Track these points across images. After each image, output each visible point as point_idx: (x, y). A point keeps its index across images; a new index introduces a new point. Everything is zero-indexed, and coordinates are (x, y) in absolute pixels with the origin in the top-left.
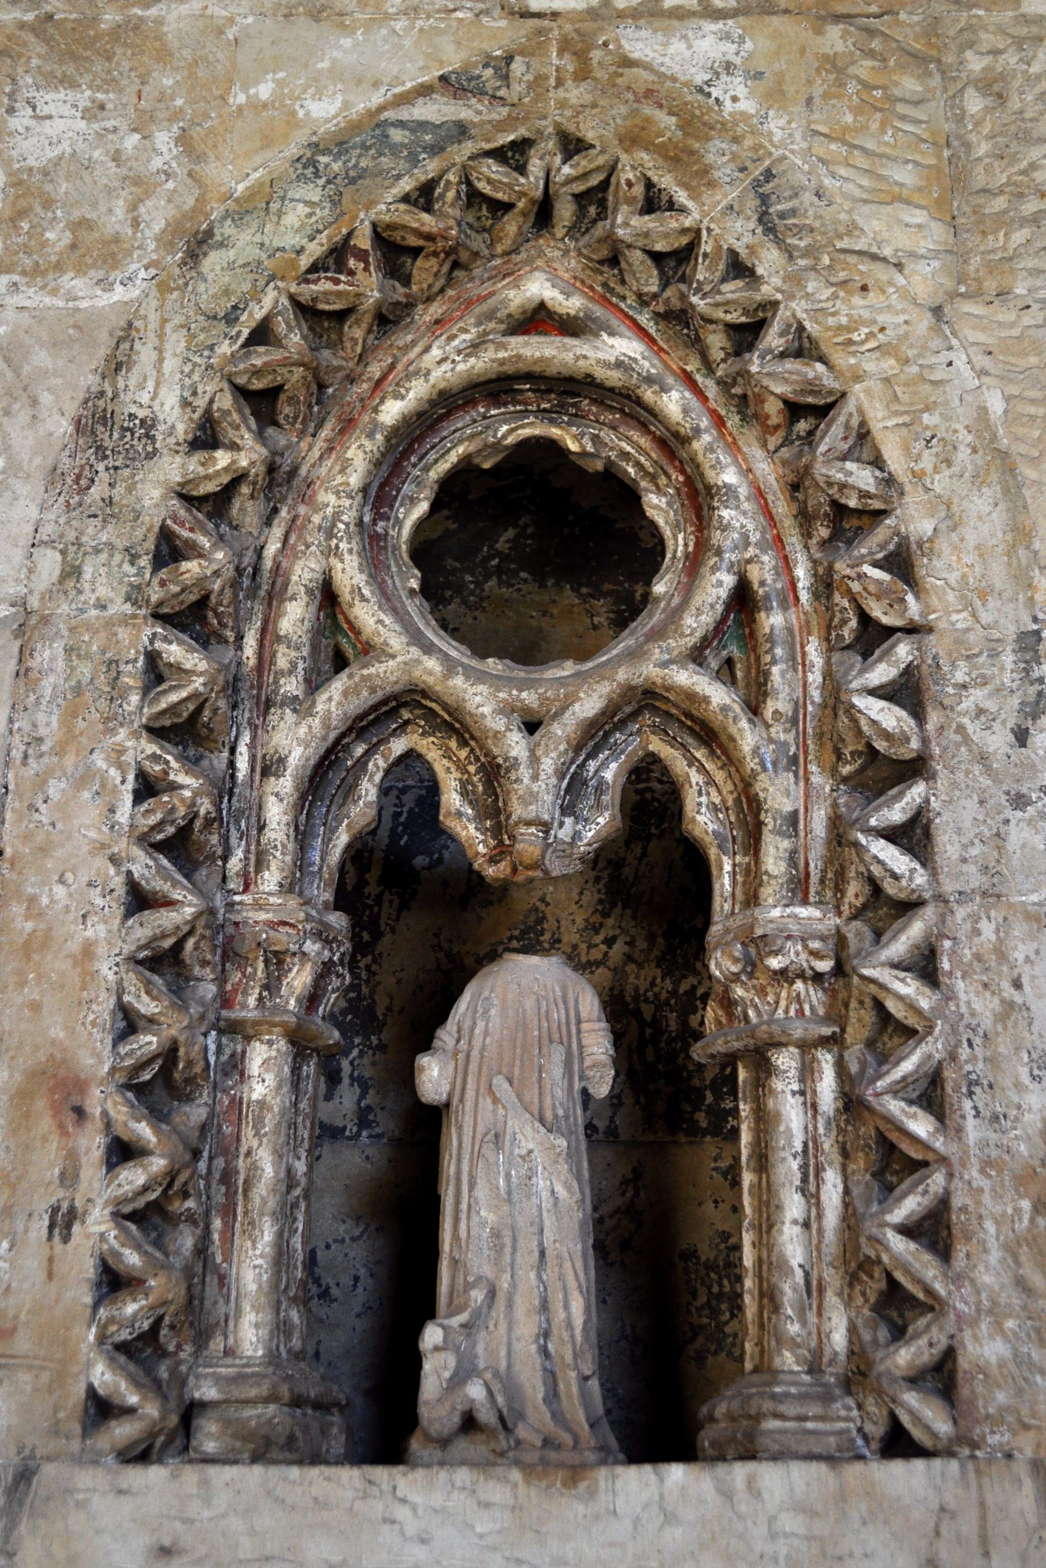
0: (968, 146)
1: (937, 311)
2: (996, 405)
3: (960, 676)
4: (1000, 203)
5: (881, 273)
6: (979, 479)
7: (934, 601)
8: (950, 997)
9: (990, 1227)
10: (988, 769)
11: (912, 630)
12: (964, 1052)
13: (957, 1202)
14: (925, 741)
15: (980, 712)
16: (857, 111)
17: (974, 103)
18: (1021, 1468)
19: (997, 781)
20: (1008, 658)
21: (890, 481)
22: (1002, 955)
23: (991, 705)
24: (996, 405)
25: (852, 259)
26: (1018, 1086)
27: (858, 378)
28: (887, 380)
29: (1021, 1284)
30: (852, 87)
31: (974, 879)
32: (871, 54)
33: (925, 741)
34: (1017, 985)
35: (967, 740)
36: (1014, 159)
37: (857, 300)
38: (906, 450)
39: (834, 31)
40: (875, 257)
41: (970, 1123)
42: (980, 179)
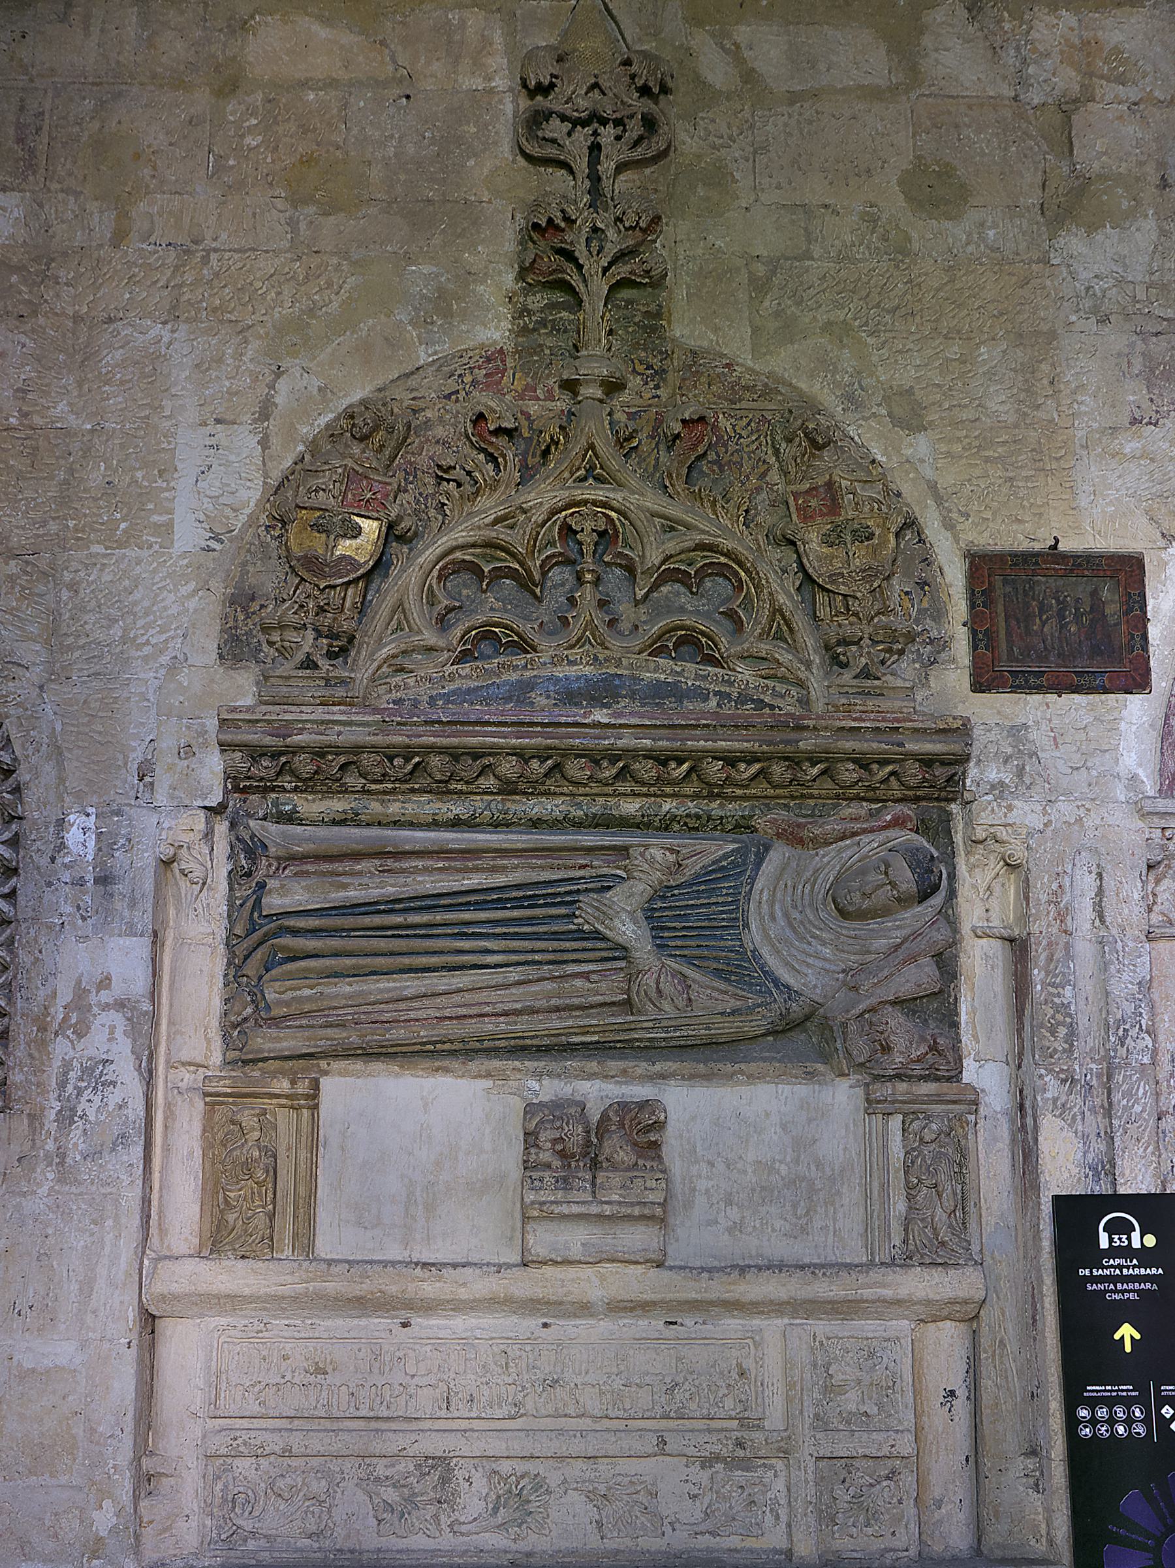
0: (60, 614)
1: (41, 687)
2: (59, 728)
3: (33, 837)
4: (71, 639)
5: (21, 672)
6: (49, 758)
7: (27, 807)
8: (17, 956)
9: (22, 1036)
10: (39, 873)
11: (20, 818)
12: (19, 976)
13: (11, 1028)
14: (18, 862)
15: (39, 850)
16: (17, 600)
17: (65, 595)
18: (24, 1116)
19: (42, 877)
20: (51, 830)
21: (15, 759)
22: (36, 940)
23: (43, 848)
24: (59, 728)
25: (10, 666)
26: (37, 988)
27: (7, 717)
28: (18, 717)
29: (31, 1056)
30: (18, 588)
31: (31, 914)
32: (26, 573)
33: (18, 862)
34: (40, 952)
35: (33, 861)
36: (79, 620)
37: (11, 684)
38: (23, 746)
39: (13, 563)
40: (19, 665)
41: (19, 1000)
42: (65, 630)
